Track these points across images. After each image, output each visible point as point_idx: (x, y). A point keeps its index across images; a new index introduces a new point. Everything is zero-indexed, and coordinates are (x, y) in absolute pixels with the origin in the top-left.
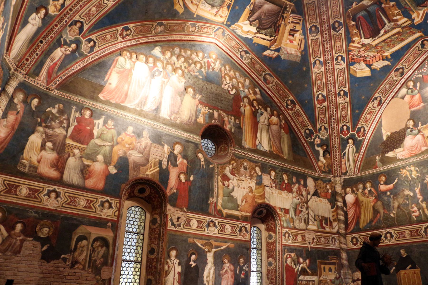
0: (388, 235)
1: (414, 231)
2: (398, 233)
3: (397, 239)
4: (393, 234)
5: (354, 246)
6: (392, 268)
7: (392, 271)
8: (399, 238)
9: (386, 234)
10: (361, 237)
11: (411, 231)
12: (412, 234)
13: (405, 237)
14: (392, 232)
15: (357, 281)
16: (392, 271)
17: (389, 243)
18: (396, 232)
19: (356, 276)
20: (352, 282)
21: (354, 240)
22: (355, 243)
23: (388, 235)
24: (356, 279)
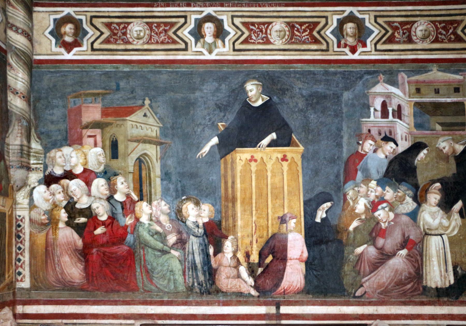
0: (209, 28)
1: (301, 24)
2: (244, 24)
3: (237, 47)
4: (226, 27)
5: (63, 50)
6: (209, 140)
7: (206, 149)
8: (246, 41)
9: (200, 24)
10: (95, 21)
11: (291, 26)
12: (293, 34)
13: (268, 42)
14: (225, 18)
15: (65, 182)
16: (206, 149)
17: (208, 57)
18: (237, 21)
19: (59, 160)
20: (40, 183)
21: (68, 28)
22: (68, 39)
23: (209, 28)
24: (58, 171)
